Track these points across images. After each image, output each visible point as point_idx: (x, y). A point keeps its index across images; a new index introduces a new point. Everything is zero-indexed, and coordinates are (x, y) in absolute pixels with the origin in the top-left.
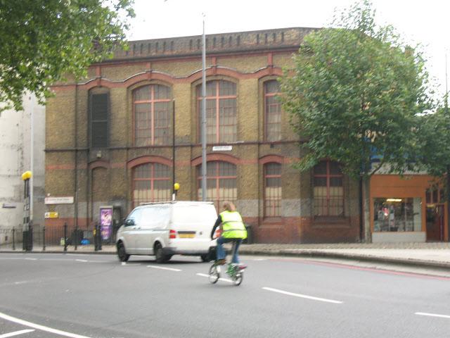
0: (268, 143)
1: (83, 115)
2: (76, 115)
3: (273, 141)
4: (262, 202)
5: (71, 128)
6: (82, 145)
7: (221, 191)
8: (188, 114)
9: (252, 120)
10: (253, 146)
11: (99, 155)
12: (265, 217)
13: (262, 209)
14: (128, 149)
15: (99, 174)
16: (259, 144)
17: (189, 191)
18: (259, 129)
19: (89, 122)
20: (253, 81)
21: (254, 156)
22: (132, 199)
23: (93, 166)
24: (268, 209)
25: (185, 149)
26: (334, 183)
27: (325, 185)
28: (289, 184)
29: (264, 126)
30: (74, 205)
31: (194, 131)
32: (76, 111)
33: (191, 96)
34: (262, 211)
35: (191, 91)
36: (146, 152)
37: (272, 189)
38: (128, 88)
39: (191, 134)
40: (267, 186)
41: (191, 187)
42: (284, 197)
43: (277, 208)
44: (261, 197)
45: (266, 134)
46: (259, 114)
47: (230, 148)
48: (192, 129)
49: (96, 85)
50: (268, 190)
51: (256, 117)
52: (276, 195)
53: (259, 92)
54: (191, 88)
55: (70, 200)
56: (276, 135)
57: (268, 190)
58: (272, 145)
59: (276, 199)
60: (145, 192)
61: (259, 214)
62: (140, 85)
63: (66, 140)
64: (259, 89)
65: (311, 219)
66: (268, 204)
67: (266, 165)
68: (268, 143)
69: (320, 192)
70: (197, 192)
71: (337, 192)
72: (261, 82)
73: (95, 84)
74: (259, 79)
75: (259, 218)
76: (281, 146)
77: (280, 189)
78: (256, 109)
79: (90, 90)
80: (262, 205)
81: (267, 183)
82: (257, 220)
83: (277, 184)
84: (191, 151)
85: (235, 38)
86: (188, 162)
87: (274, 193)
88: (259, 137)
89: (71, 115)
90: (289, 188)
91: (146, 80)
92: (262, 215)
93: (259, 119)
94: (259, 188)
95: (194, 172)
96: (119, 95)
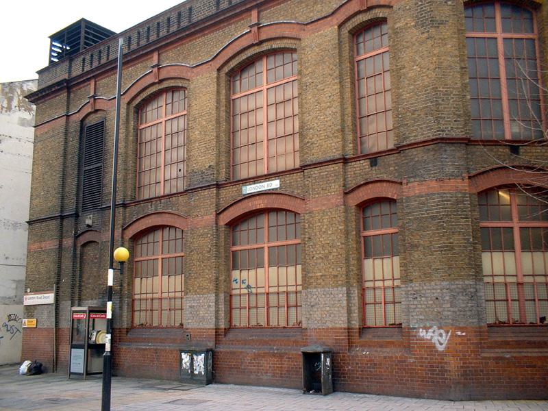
0: (364, 157)
1: (73, 160)
2: (64, 164)
3: (375, 150)
4: (355, 293)
5: (57, 182)
6: (70, 208)
7: (527, 258)
8: (211, 126)
9: (328, 112)
10: (331, 168)
11: (89, 222)
12: (363, 329)
13: (355, 309)
14: (218, 186)
15: (90, 252)
16: (345, 161)
17: (212, 276)
18: (343, 130)
19: (79, 170)
20: (329, 31)
21: (336, 188)
22: (131, 295)
23: (82, 240)
24: (235, 313)
25: (206, 192)
26: (280, 258)
27: (511, 248)
28: (417, 246)
29: (355, 120)
30: (54, 307)
31: (223, 159)
32: (65, 156)
33: (218, 93)
34: (356, 315)
35: (218, 85)
36: (150, 209)
37: (378, 262)
38: (219, 70)
39: (218, 163)
40: (367, 255)
41: (218, 267)
42: (406, 279)
43: (390, 307)
44: (354, 282)
45: (359, 139)
46: (342, 97)
47: (275, 184)
48: (219, 155)
49: (90, 110)
50: (368, 263)
51: (336, 107)
52: (388, 275)
53: (340, 55)
54: (218, 78)
55: (49, 298)
56: (379, 137)
57: (368, 263)
58: (374, 159)
59: (172, 295)
60: (252, 273)
61: (349, 322)
62: (144, 95)
63: (51, 204)
64: (340, 43)
65: (479, 331)
66: (369, 297)
67: (364, 206)
68: (364, 157)
69: (496, 263)
70: (229, 276)
71: (290, 276)
72: (345, 31)
73: (88, 109)
74: (340, 26)
75: (349, 330)
76: (392, 159)
77: (396, 259)
78: (337, 87)
79: (82, 121)
80: (355, 300)
81: (367, 249)
82: (344, 336)
83: (392, 248)
84: (218, 195)
85: (174, 16)
86: (211, 218)
87: (381, 270)
88: (344, 147)
89: (58, 164)
90: (417, 255)
91: (153, 84)
92: (356, 324)
93: (343, 110)
94: (347, 260)
95: (222, 236)
96: (114, 115)
